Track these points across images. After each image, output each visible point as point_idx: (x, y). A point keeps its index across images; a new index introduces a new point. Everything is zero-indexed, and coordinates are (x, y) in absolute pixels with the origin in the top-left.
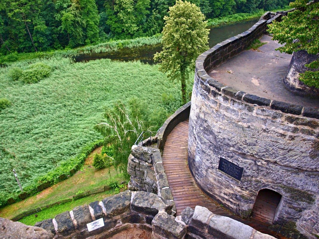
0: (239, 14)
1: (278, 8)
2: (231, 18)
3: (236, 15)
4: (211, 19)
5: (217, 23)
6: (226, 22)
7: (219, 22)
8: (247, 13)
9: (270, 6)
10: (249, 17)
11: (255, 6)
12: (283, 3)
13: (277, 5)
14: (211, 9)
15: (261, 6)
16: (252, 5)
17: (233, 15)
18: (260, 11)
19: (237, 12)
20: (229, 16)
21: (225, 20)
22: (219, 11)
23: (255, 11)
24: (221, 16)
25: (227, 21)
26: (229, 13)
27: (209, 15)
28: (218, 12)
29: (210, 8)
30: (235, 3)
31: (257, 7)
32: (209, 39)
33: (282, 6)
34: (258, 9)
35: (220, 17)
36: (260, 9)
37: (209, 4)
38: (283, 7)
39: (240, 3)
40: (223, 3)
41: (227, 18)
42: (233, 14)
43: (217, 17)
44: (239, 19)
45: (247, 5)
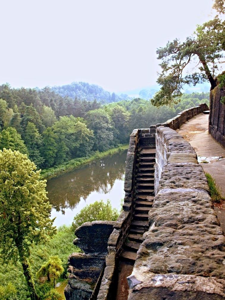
0: (75, 159)
1: (112, 148)
2: (68, 165)
3: (73, 161)
4: (46, 170)
5: (54, 173)
6: (63, 170)
7: (55, 172)
8: (84, 157)
9: (104, 147)
10: (86, 161)
11: (89, 149)
12: (115, 142)
13: (110, 145)
14: (44, 159)
15: (95, 148)
16: (86, 149)
17: (69, 162)
18: (96, 153)
19: (73, 158)
20: (65, 163)
21: (61, 168)
22: (53, 159)
23: (91, 154)
24: (56, 165)
25: (64, 168)
26: (65, 160)
27: (43, 166)
28: (52, 161)
29: (42, 158)
30: (68, 149)
31: (91, 150)
32: (47, 192)
33: (116, 146)
34: (93, 151)
35: (55, 166)
36: (94, 151)
37: (40, 154)
38: (117, 146)
39: (73, 148)
40: (56, 151)
41: (63, 165)
42: (69, 160)
43: (52, 166)
44: (77, 164)
45: (81, 149)
